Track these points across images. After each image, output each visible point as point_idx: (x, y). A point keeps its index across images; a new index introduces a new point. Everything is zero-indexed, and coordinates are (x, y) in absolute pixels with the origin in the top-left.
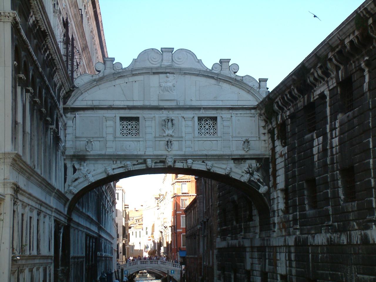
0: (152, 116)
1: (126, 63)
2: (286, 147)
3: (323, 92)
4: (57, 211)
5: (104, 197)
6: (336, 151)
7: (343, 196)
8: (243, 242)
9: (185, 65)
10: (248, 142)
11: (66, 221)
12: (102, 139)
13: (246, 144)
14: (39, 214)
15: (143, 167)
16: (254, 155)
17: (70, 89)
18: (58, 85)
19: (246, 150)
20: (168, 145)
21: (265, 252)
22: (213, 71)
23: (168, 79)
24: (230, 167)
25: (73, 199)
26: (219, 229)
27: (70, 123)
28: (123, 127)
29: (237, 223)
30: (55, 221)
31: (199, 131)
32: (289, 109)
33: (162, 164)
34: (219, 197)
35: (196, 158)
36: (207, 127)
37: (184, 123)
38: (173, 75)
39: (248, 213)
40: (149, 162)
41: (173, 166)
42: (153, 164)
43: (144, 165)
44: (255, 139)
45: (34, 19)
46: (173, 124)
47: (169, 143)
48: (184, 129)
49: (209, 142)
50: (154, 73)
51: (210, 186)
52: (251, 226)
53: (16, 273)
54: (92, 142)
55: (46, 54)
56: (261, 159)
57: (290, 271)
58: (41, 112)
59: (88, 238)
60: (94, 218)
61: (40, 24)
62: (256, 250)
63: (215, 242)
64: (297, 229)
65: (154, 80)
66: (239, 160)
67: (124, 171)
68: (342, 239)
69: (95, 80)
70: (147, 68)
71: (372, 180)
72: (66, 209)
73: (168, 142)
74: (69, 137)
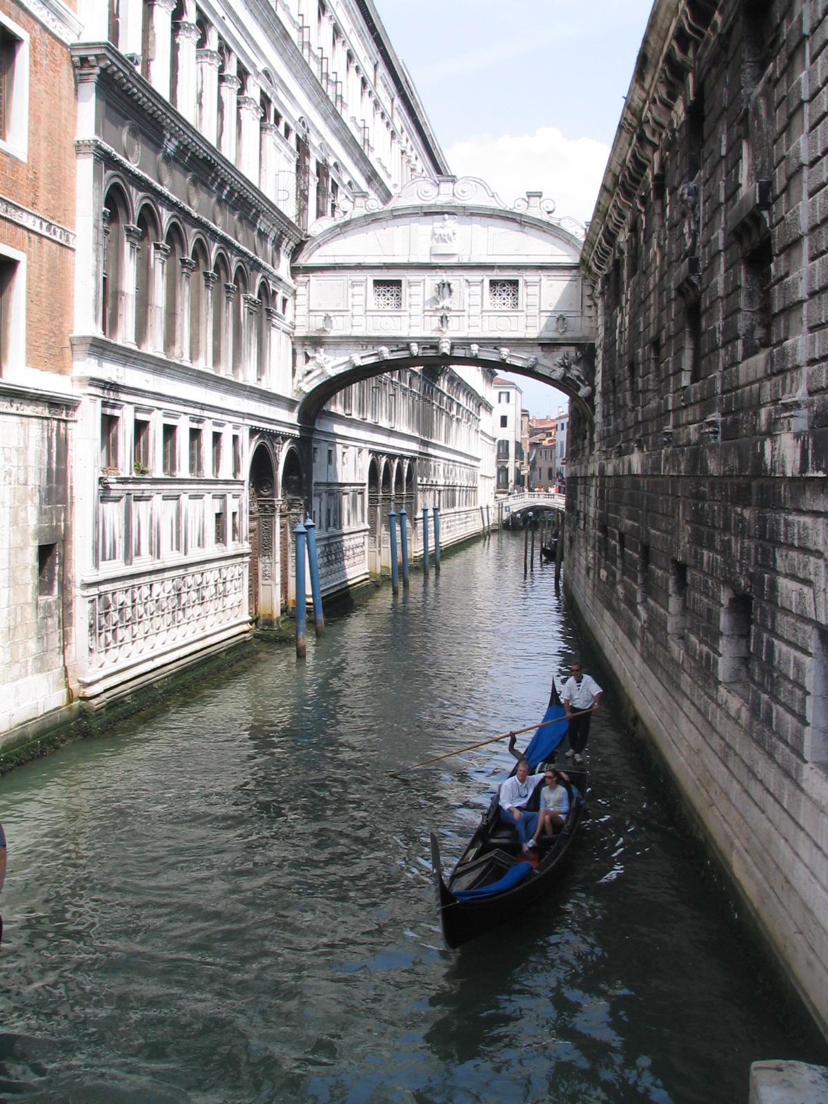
0: (421, 278)
4: (251, 416)
5: (445, 398)
11: (297, 433)
13: (561, 322)
16: (572, 339)
18: (272, 235)
19: (561, 331)
22: (515, 211)
23: (446, 223)
27: (301, 290)
30: (254, 432)
33: (434, 351)
35: (484, 342)
37: (467, 290)
40: (415, 349)
42: (421, 351)
43: (407, 352)
45: (176, 143)
47: (444, 319)
48: (467, 299)
50: (426, 214)
53: (123, 501)
55: (225, 192)
58: (206, 274)
60: (405, 429)
61: (193, 150)
66: (547, 345)
69: (337, 226)
71: (640, 380)
74: (300, 310)
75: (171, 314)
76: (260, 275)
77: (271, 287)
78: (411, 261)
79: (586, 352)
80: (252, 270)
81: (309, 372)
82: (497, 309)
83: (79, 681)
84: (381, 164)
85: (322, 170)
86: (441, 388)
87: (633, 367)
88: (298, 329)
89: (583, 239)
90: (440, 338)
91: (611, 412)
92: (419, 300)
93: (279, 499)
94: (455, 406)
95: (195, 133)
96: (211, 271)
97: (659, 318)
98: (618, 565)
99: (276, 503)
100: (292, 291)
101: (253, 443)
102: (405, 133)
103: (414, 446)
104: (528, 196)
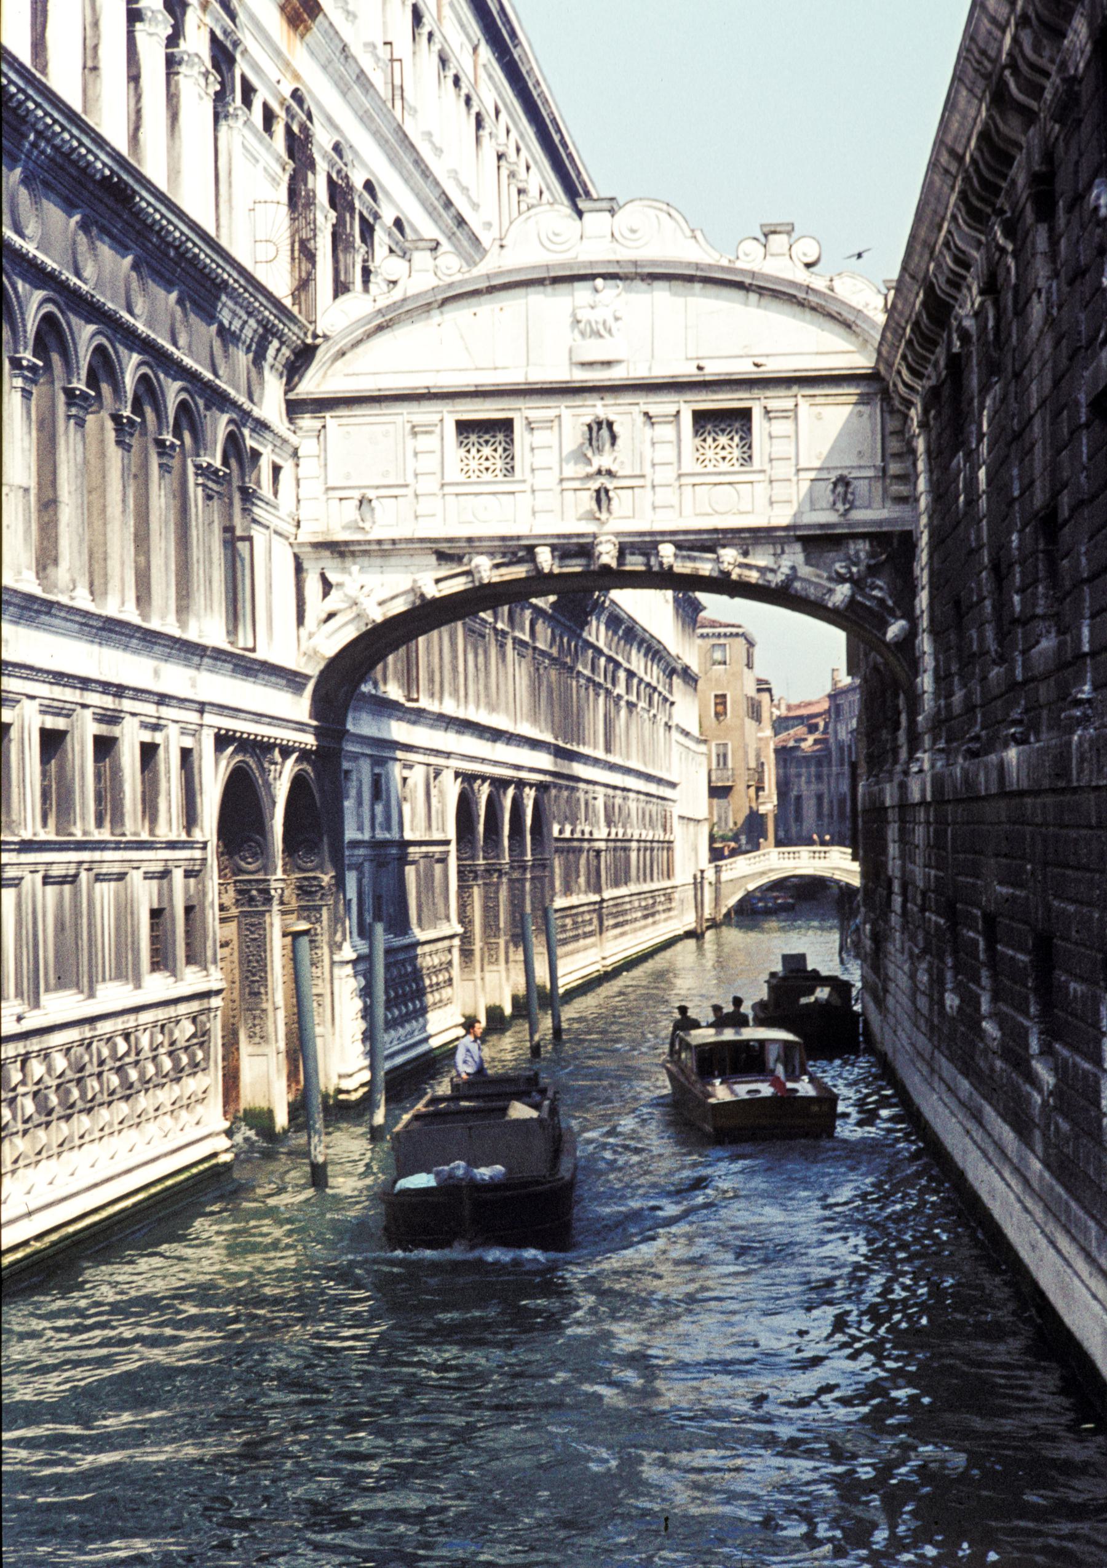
0: (551, 413)
5: (603, 660)
10: (847, 484)
13: (840, 489)
17: (303, 342)
22: (739, 265)
23: (599, 296)
24: (790, 564)
25: (322, 672)
27: (308, 446)
28: (468, 451)
31: (697, 455)
32: (929, 378)
33: (583, 561)
38: (611, 283)
41: (614, 564)
42: (557, 561)
44: (871, 473)
47: (601, 497)
50: (556, 280)
54: (374, 503)
59: (487, 784)
67: (470, 586)
71: (1016, 598)
73: (598, 491)
75: (48, 504)
76: (225, 418)
77: (250, 443)
78: (531, 379)
80: (208, 408)
81: (331, 616)
82: (710, 469)
84: (459, 183)
85: (339, 194)
86: (592, 639)
87: (1000, 571)
89: (881, 318)
90: (595, 536)
91: (954, 668)
92: (550, 458)
93: (279, 878)
94: (622, 675)
95: (86, 129)
96: (127, 412)
97: (1054, 468)
98: (985, 981)
99: (274, 885)
100: (291, 450)
101: (223, 763)
102: (503, 115)
103: (544, 760)
104: (766, 235)
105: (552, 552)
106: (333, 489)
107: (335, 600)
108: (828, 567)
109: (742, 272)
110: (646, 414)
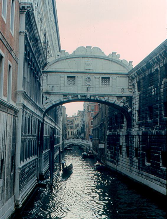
0: (81, 76)
1: (70, 53)
2: (140, 92)
3: (157, 68)
4: (39, 116)
6: (162, 95)
7: (164, 114)
8: (119, 133)
9: (97, 54)
10: (123, 89)
12: (59, 86)
13: (122, 90)
14: (32, 117)
15: (76, 98)
18: (41, 61)
20: (88, 89)
21: (129, 137)
22: (109, 57)
25: (45, 111)
26: (108, 127)
27: (45, 78)
29: (117, 124)
33: (85, 97)
34: (109, 113)
36: (105, 82)
38: (90, 58)
39: (122, 120)
44: (127, 88)
46: (90, 80)
47: (88, 89)
49: (106, 89)
50: (83, 57)
51: (105, 108)
52: (123, 126)
56: (129, 97)
57: (140, 146)
58: (34, 73)
60: (53, 120)
62: (124, 136)
63: (107, 132)
64: (143, 128)
65: (83, 61)
66: (119, 97)
68: (162, 132)
70: (80, 55)
72: (43, 115)
79: (130, 99)
83: (16, 200)
88: (44, 90)
90: (87, 94)
98: (161, 161)
103: (53, 125)
105: (81, 95)
106: (48, 85)
107: (48, 101)
108: (120, 101)
109: (110, 58)
110: (95, 77)
